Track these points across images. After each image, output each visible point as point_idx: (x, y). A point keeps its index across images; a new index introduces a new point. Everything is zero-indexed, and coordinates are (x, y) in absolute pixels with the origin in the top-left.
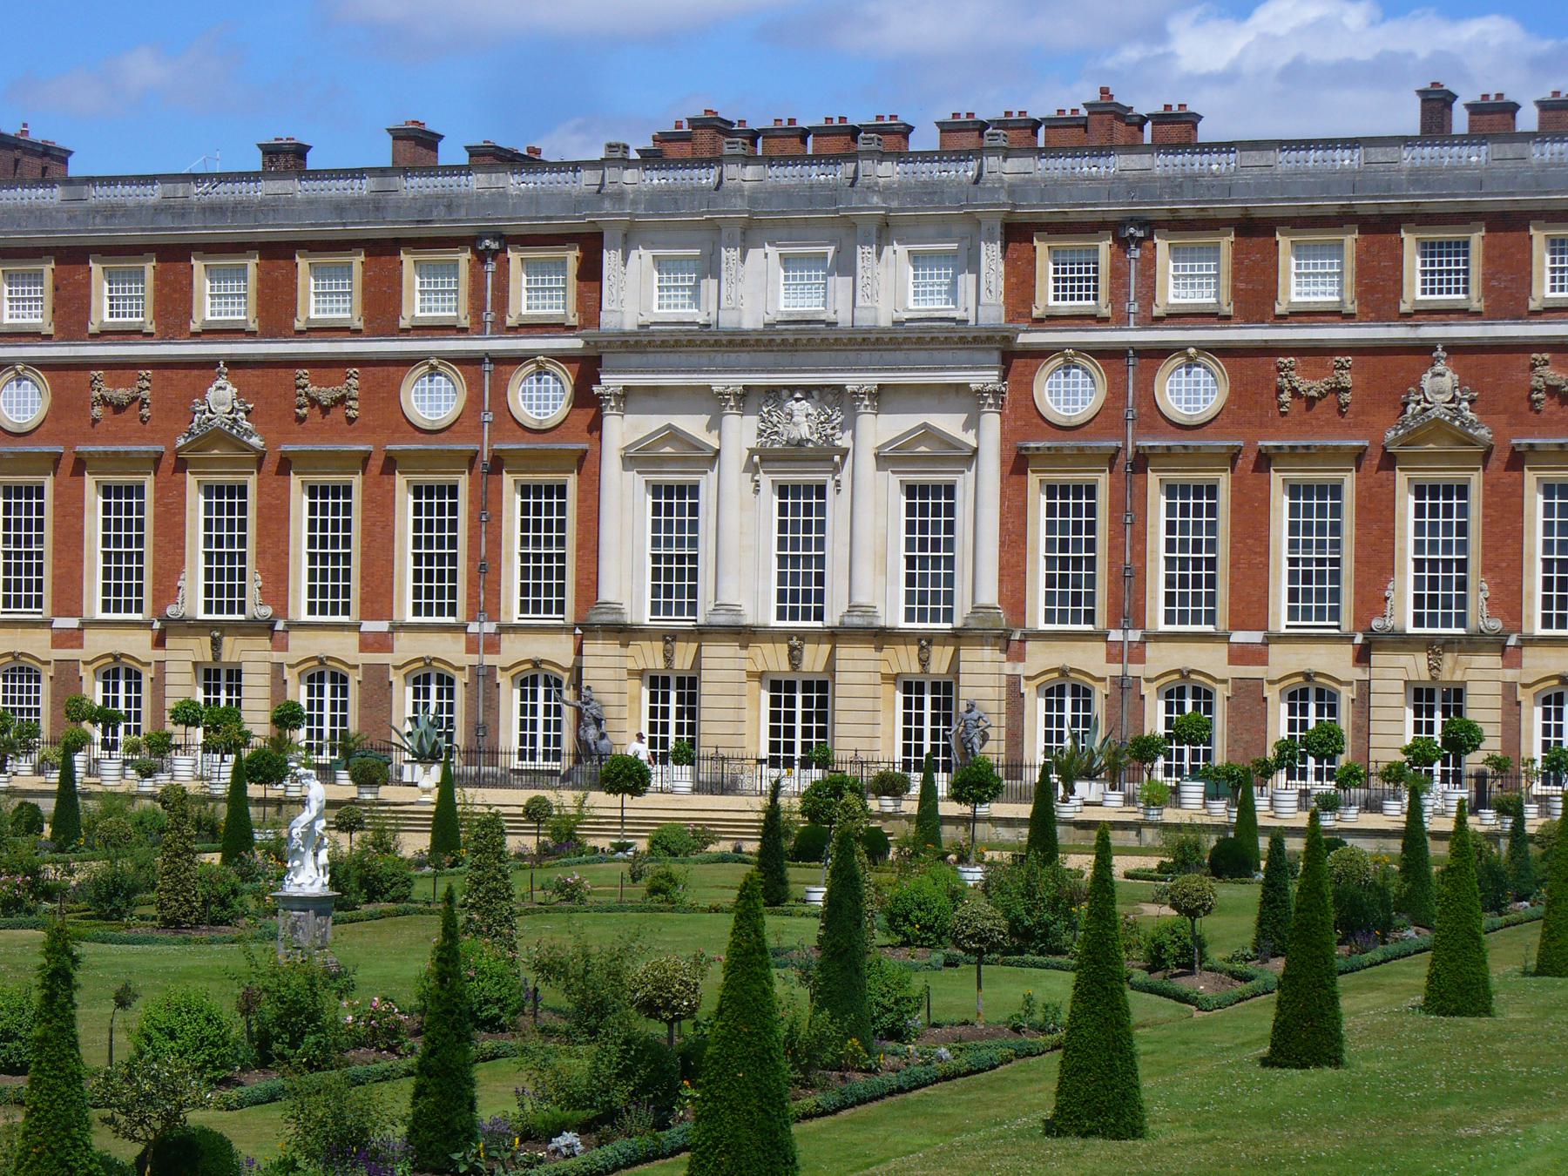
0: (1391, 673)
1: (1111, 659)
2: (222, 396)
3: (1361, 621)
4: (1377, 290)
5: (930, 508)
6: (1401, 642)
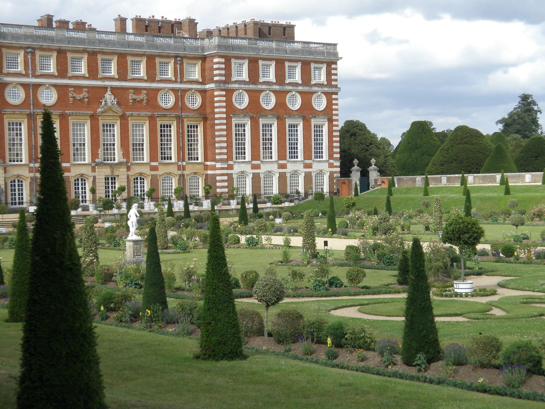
0: (102, 174)
1: (279, 168)
3: (93, 160)
4: (93, 73)
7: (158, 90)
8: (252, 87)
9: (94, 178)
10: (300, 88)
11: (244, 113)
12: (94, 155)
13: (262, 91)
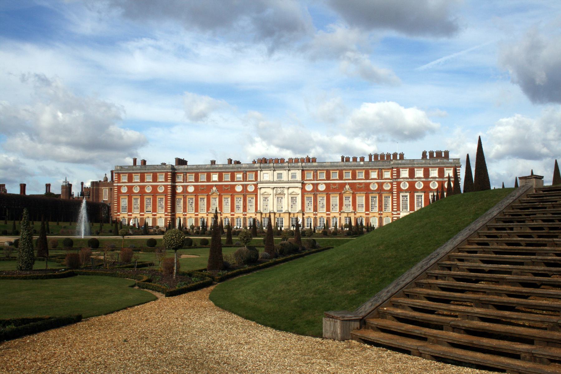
2: (214, 189)
3: (340, 210)
4: (341, 177)
5: (293, 200)
6: (344, 212)
7: (370, 183)
8: (410, 180)
9: (340, 218)
10: (437, 179)
11: (406, 191)
12: (341, 208)
13: (416, 181)
